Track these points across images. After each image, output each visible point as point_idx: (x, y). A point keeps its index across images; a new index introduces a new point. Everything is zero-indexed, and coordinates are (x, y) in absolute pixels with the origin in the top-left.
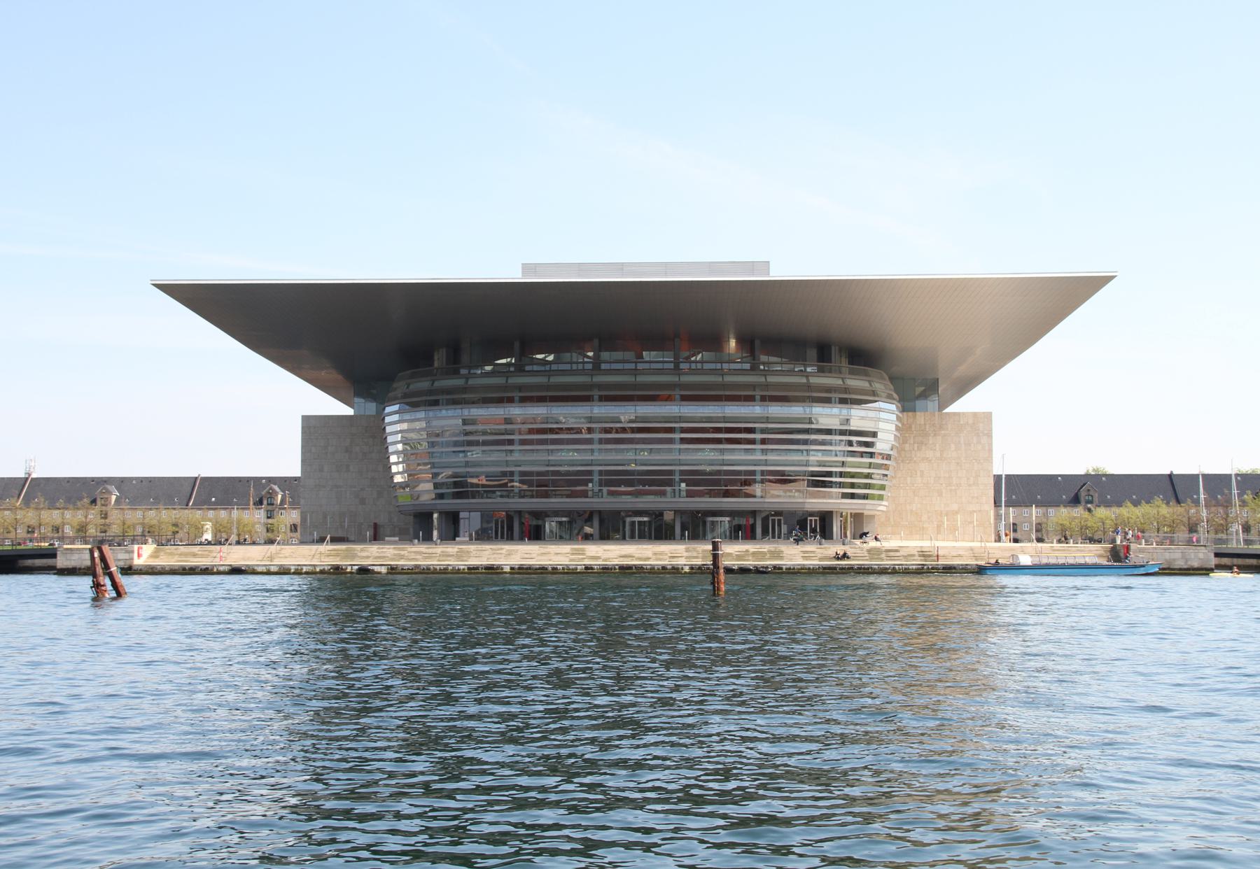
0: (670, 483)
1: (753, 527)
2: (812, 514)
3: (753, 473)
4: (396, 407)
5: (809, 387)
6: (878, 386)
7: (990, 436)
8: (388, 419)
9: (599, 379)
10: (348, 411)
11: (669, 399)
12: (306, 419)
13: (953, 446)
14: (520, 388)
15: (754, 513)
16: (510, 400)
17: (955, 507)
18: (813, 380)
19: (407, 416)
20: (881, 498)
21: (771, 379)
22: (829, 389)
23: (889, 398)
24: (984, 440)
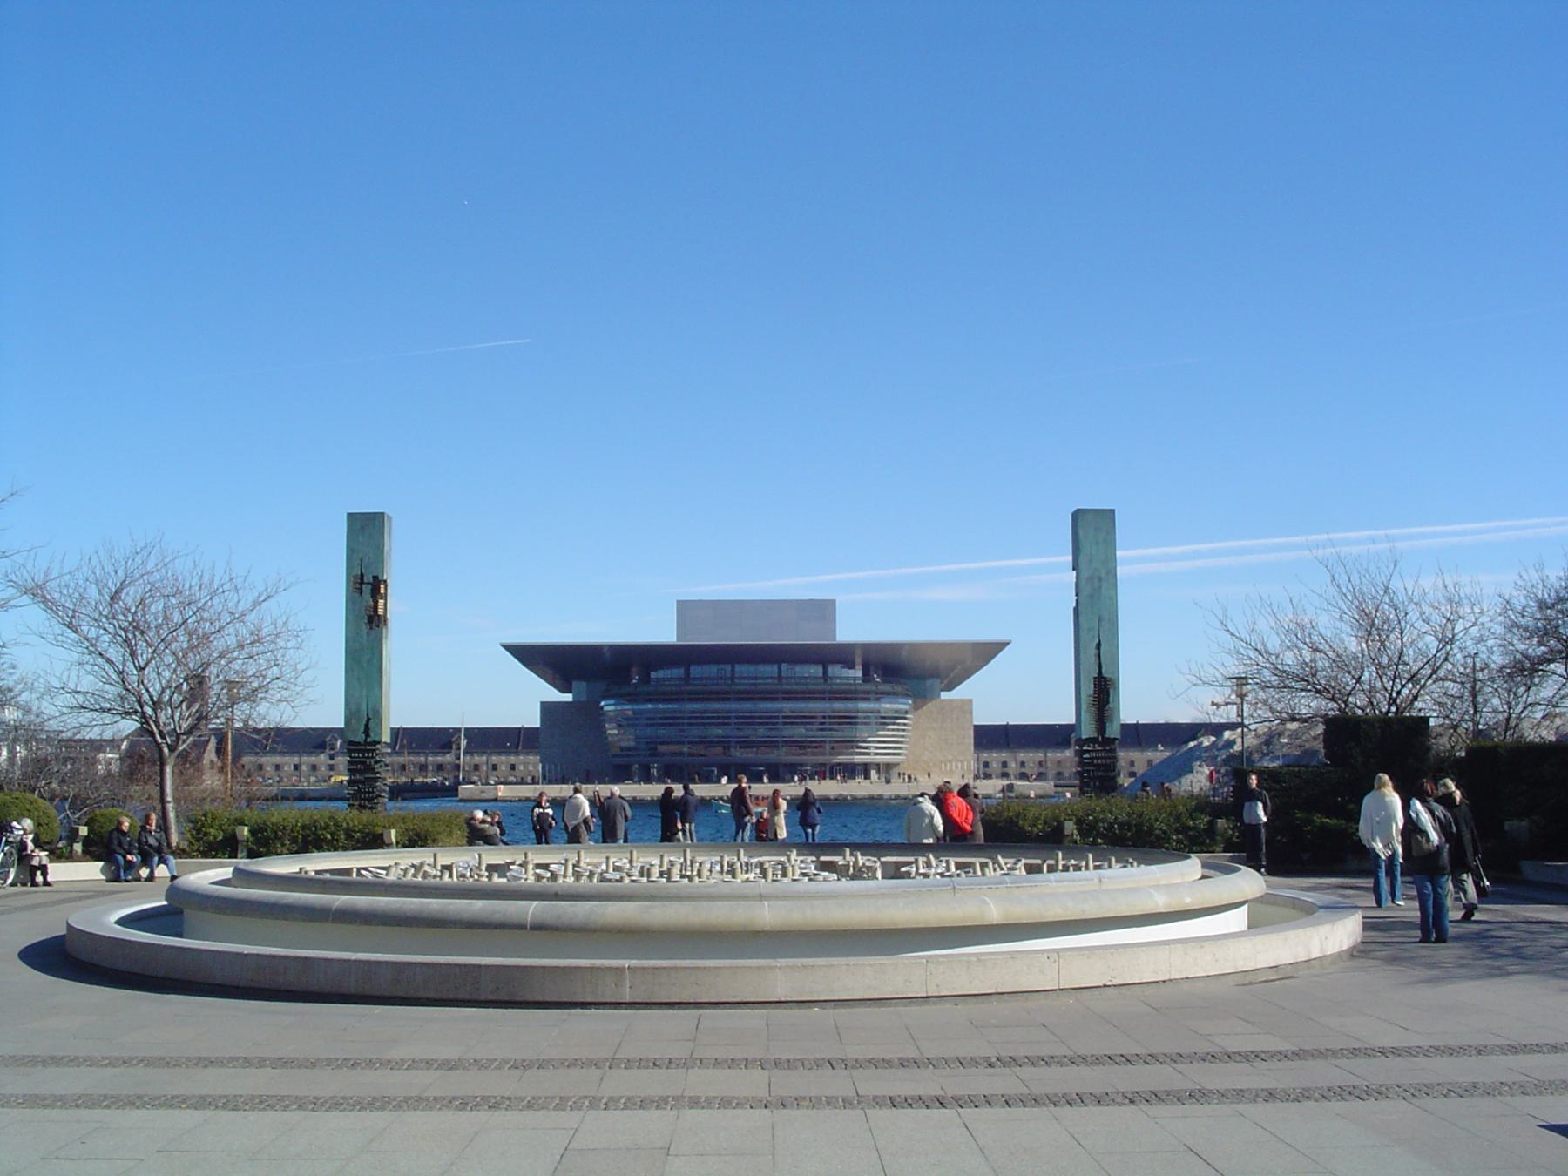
0: (777, 747)
1: (824, 773)
2: (859, 764)
3: (824, 742)
4: (612, 702)
5: (855, 692)
6: (898, 688)
7: (971, 713)
8: (606, 708)
9: (733, 687)
10: (568, 697)
11: (775, 699)
12: (543, 704)
13: (948, 720)
14: (690, 693)
15: (824, 765)
16: (683, 700)
17: (950, 757)
18: (859, 688)
19: (619, 708)
20: (899, 754)
21: (834, 687)
22: (868, 693)
23: (907, 696)
24: (968, 716)
